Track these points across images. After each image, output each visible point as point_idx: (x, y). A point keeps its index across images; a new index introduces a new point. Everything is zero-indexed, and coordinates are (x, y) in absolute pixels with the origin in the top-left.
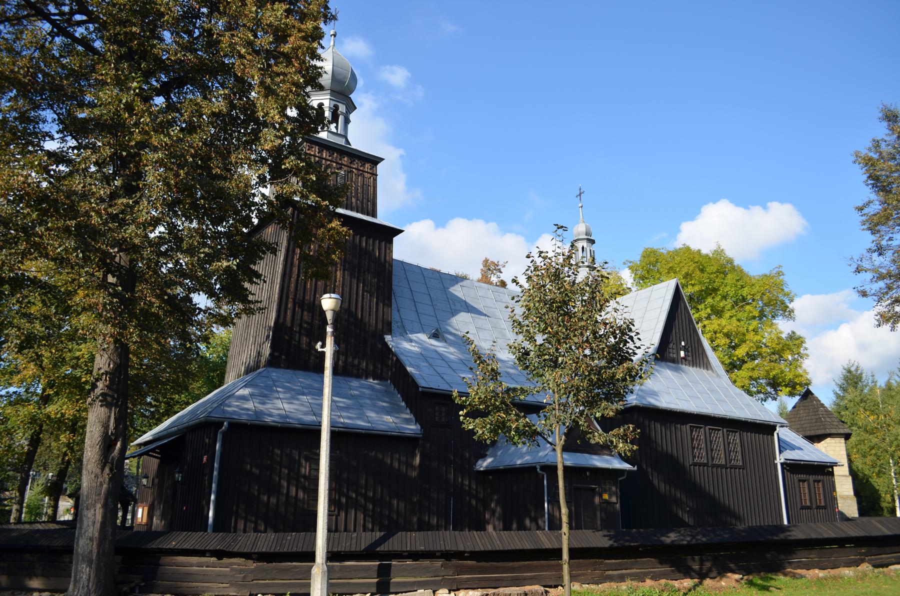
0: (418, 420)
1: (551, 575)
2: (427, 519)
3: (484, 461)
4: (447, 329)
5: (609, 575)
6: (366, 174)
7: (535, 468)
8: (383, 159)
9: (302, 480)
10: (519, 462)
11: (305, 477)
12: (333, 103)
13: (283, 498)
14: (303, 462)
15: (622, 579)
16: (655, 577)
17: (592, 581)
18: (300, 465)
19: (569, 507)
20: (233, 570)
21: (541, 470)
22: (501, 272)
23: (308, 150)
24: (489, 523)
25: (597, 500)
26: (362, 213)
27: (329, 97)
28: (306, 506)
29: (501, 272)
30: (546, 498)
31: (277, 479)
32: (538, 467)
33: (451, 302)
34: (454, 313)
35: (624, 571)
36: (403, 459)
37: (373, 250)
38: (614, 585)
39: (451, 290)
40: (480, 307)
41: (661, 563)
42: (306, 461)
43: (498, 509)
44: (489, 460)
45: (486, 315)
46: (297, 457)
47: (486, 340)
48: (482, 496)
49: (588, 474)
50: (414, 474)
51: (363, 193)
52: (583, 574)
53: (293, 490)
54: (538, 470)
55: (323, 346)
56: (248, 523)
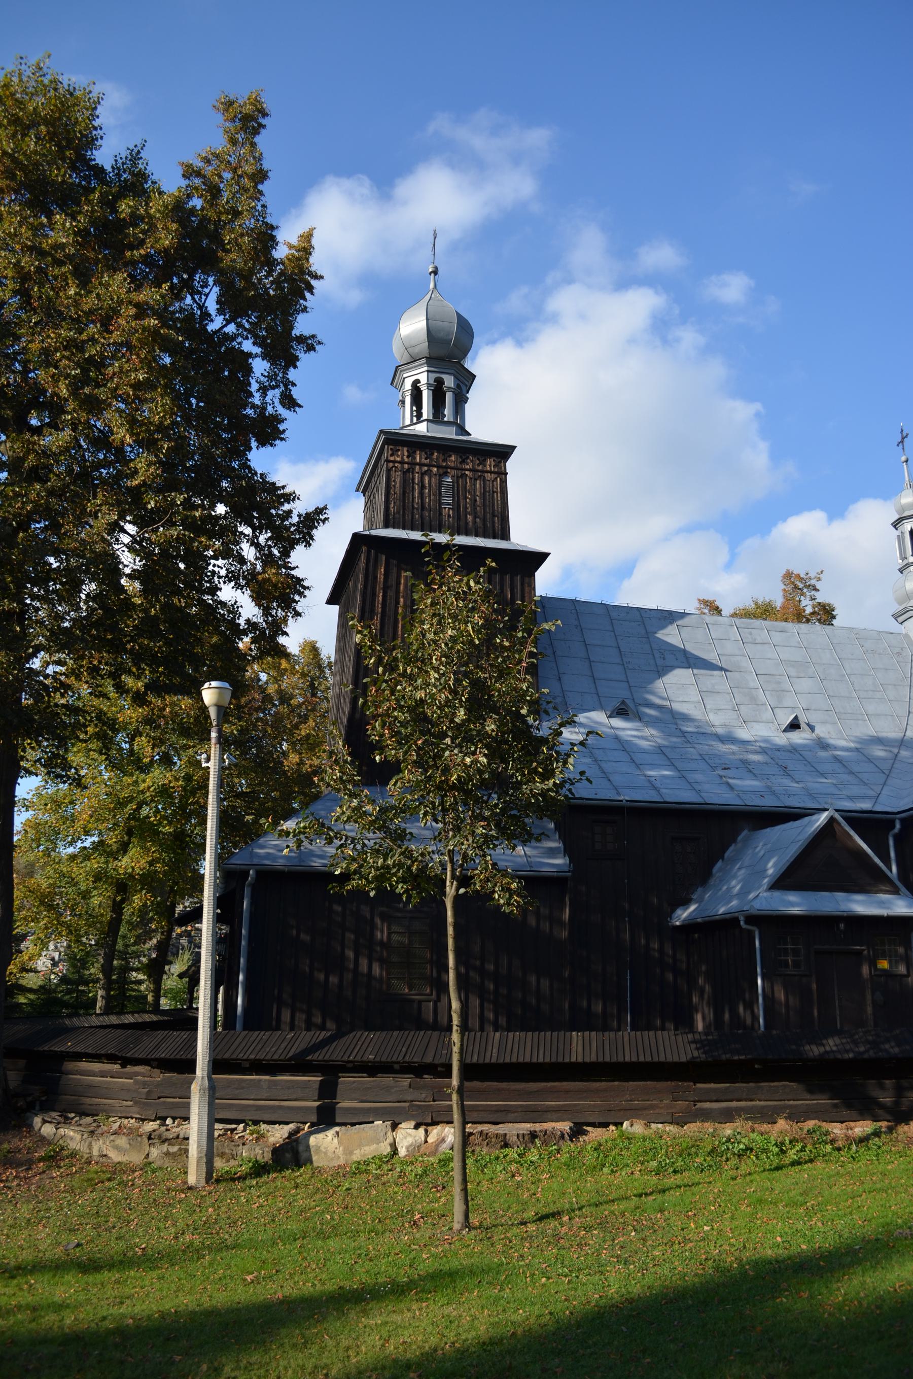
0: (568, 850)
1: (594, 1106)
2: (585, 1004)
3: (687, 909)
4: (646, 700)
5: (701, 1109)
6: (488, 476)
7: (736, 920)
8: (514, 447)
9: (378, 949)
10: (721, 911)
11: (382, 943)
13: (349, 976)
14: (378, 921)
15: (727, 1116)
16: (796, 1116)
17: (669, 1118)
18: (373, 926)
19: (460, 999)
20: (136, 1082)
21: (746, 922)
22: (817, 590)
23: (392, 455)
24: (697, 1011)
25: (865, 970)
26: (485, 536)
27: (426, 368)
28: (384, 987)
29: (817, 590)
30: (759, 970)
31: (339, 949)
32: (742, 919)
33: (657, 655)
34: (662, 671)
35: (734, 1104)
36: (544, 911)
37: (502, 590)
38: (709, 1127)
39: (660, 635)
40: (712, 657)
41: (811, 1092)
42: (383, 920)
43: (708, 988)
44: (692, 908)
45: (721, 669)
46: (368, 916)
47: (717, 710)
48: (684, 966)
49: (842, 926)
50: (564, 934)
51: (484, 505)
52: (652, 1107)
53: (364, 963)
54: (742, 923)
55: (208, 760)
56: (298, 1015)
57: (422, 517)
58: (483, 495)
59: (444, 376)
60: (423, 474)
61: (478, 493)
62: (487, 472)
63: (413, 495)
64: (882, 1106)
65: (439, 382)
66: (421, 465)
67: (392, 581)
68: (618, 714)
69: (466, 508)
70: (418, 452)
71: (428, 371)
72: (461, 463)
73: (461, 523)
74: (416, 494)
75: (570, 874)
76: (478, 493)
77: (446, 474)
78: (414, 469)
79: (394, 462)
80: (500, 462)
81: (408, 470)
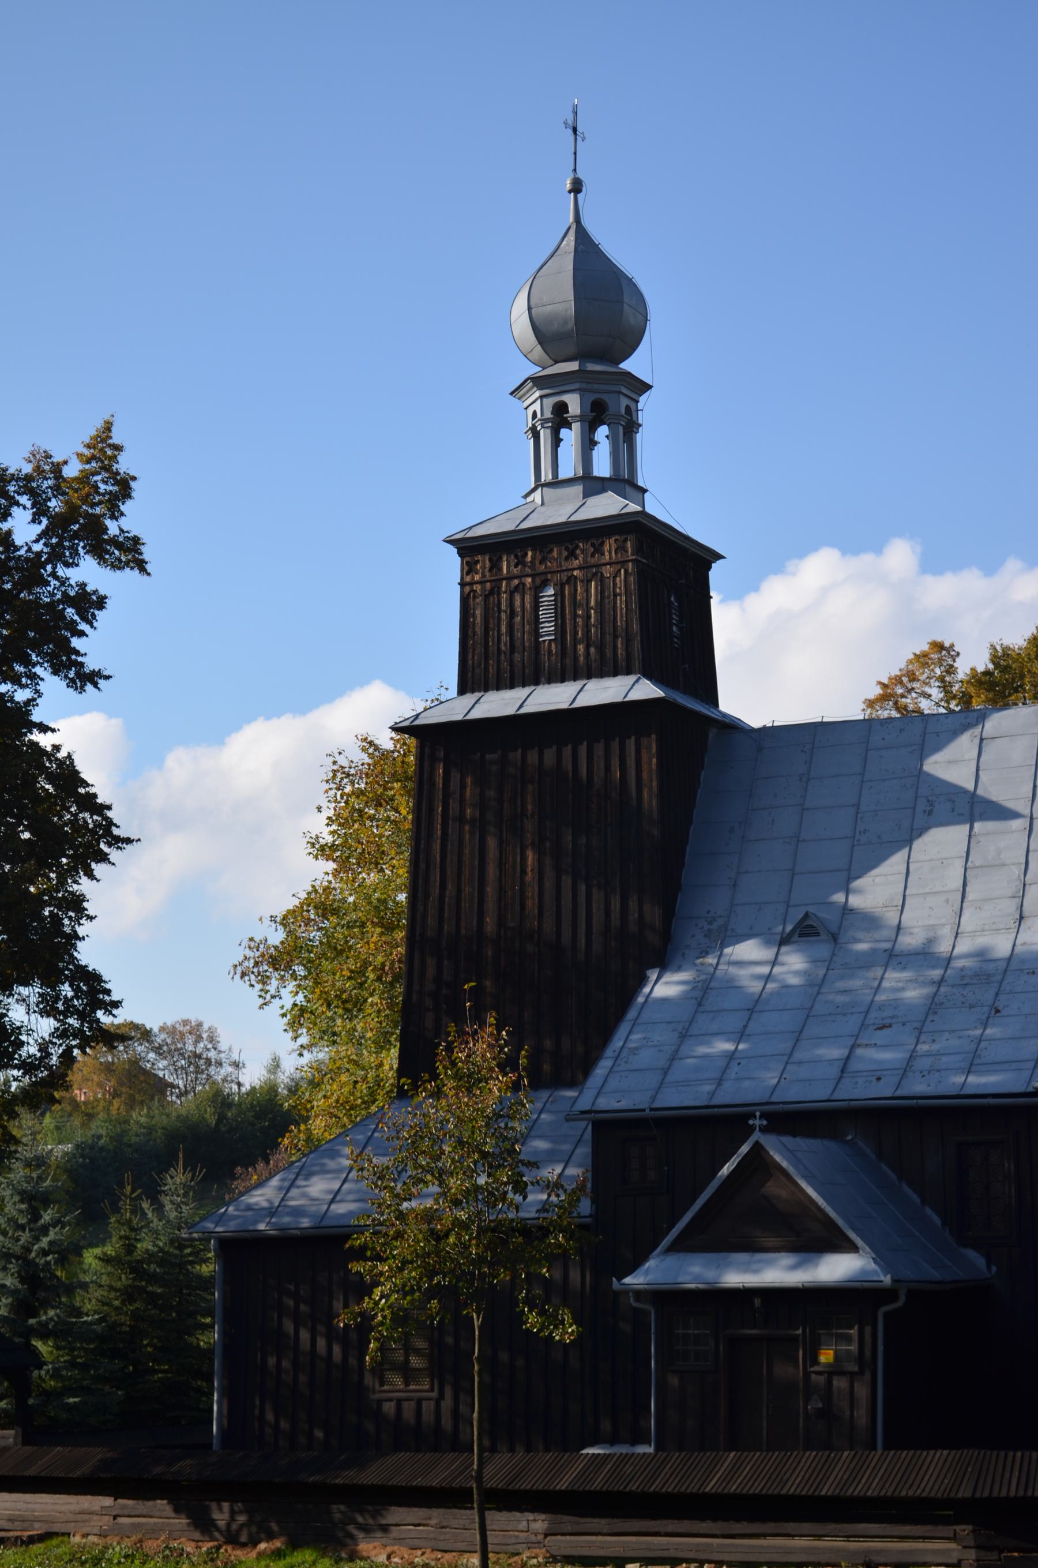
12: (550, 402)
21: (637, 1299)
49: (757, 1302)
51: (601, 621)
57: (511, 663)
58: (600, 604)
59: (567, 398)
61: (593, 603)
62: (605, 564)
63: (499, 631)
64: (218, 1530)
65: (561, 409)
66: (509, 579)
68: (800, 935)
69: (576, 633)
70: (505, 558)
71: (541, 397)
72: (567, 559)
73: (568, 661)
74: (504, 629)
75: (589, 1220)
76: (593, 603)
77: (545, 584)
78: (500, 588)
79: (471, 584)
80: (625, 541)
81: (492, 592)
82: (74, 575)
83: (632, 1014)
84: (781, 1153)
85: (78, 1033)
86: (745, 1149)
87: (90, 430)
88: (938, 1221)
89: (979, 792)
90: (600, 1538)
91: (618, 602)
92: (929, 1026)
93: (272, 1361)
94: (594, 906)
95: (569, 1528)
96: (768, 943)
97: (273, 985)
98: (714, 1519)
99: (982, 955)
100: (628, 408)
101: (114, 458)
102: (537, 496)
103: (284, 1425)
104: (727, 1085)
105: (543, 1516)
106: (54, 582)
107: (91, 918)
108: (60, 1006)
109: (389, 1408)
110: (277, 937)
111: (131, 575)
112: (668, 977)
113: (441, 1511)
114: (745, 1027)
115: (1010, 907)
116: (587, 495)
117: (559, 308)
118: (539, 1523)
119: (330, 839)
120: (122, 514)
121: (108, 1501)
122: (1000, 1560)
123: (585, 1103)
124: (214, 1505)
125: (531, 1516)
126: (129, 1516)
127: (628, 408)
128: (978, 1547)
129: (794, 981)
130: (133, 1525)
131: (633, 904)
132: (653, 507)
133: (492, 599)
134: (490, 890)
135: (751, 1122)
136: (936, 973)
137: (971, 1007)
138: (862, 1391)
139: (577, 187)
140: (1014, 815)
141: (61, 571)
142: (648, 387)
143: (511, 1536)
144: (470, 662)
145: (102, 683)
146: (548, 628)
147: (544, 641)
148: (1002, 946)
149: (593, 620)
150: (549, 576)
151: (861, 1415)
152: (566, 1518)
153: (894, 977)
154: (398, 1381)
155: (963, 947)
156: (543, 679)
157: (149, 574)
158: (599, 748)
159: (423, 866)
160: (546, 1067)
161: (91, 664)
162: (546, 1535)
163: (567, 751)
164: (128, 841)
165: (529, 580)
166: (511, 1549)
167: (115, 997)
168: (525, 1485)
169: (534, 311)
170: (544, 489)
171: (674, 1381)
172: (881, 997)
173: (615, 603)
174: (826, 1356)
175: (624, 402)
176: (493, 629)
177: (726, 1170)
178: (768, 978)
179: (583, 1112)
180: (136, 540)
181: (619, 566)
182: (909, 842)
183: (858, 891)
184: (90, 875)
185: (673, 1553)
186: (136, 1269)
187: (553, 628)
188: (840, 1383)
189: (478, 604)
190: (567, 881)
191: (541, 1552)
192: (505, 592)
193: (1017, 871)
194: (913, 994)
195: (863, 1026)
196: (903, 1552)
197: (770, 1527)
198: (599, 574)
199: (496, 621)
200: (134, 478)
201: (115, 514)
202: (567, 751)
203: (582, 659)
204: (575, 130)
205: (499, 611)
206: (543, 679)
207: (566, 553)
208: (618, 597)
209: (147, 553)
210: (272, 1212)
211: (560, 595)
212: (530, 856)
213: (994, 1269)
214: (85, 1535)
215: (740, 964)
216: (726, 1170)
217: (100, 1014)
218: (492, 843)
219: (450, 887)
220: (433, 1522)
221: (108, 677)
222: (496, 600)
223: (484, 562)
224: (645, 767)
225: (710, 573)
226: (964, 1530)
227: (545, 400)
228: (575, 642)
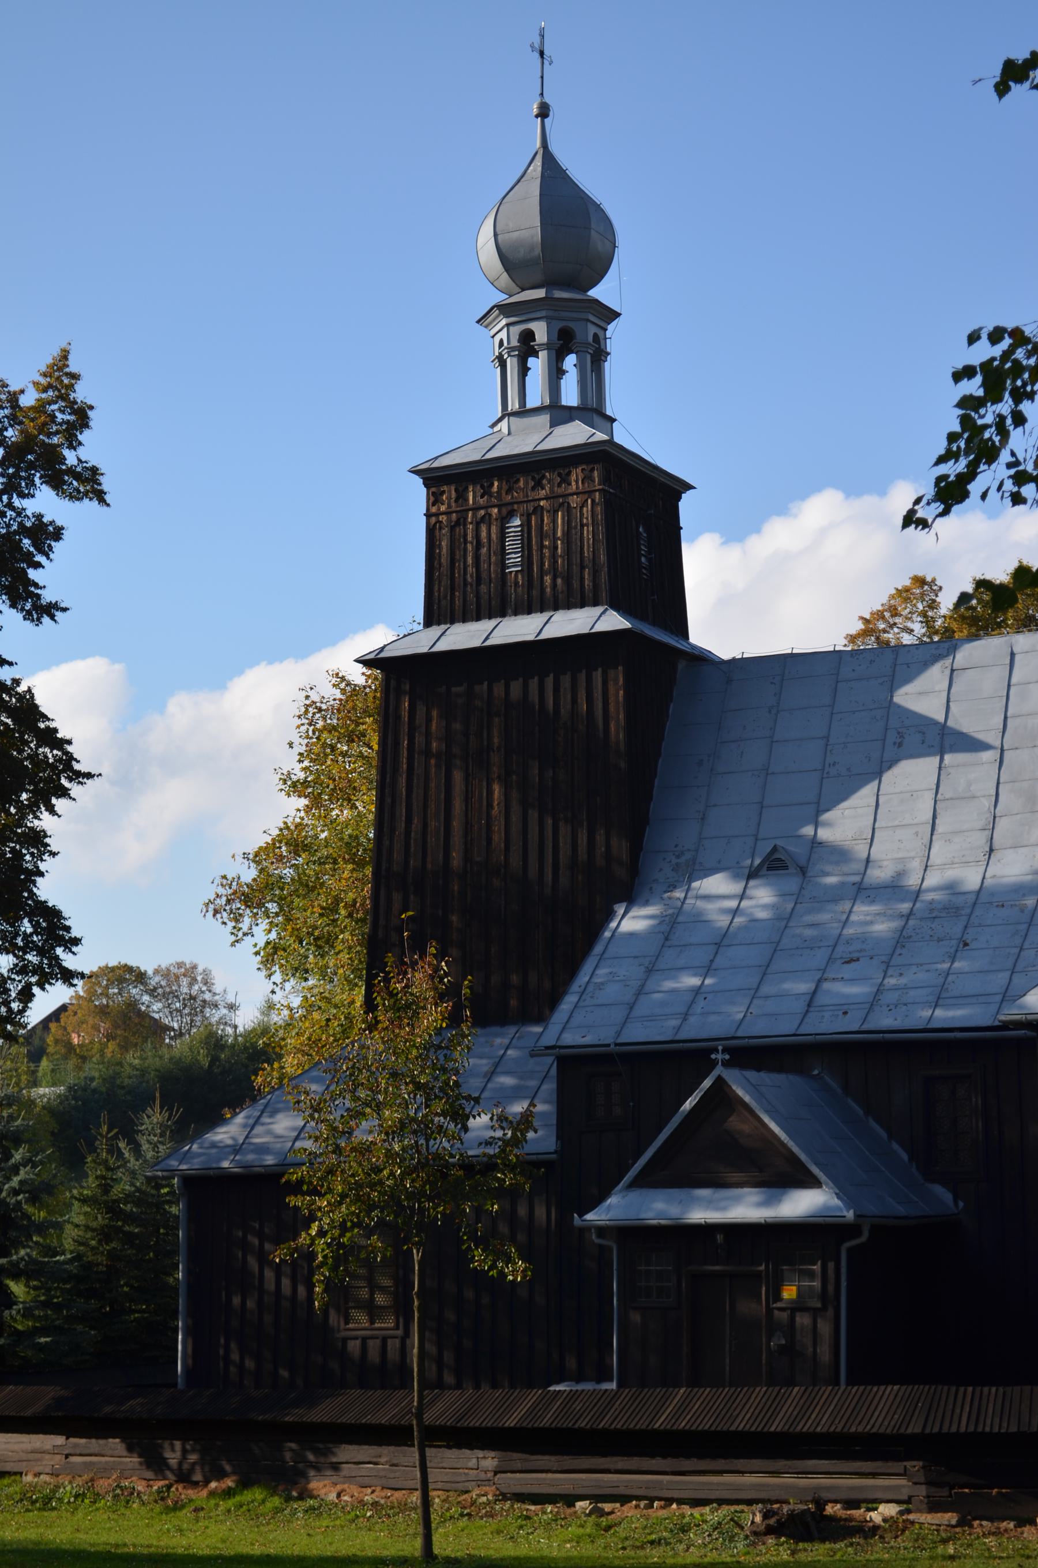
12: (516, 330)
49: (720, 1238)
51: (568, 551)
59: (534, 326)
60: (478, 525)
61: (559, 534)
64: (169, 1468)
65: (527, 337)
66: (475, 509)
67: (420, 719)
68: (769, 869)
69: (542, 564)
70: (471, 489)
71: (508, 325)
72: (533, 489)
74: (470, 560)
76: (559, 534)
77: (511, 514)
78: (466, 519)
79: (437, 515)
80: (592, 470)
81: (458, 523)
82: (31, 506)
83: (598, 949)
84: (744, 1088)
85: (38, 970)
86: (707, 1083)
87: (46, 359)
88: (905, 1157)
89: (950, 723)
90: (550, 1475)
91: (585, 532)
92: (896, 960)
93: (236, 1301)
94: (561, 839)
95: (519, 1466)
96: (736, 877)
97: (246, 923)
98: (664, 1456)
99: (951, 887)
100: (596, 336)
101: (71, 387)
102: (504, 425)
103: (250, 1364)
104: (692, 1019)
105: (493, 1454)
106: (10, 513)
107: (53, 854)
108: (19, 941)
109: (354, 1347)
110: (249, 874)
111: (89, 506)
112: (635, 912)
113: (392, 1448)
114: (712, 961)
115: (980, 839)
116: (554, 424)
117: (525, 234)
118: (489, 1460)
119: (302, 775)
120: (80, 444)
121: (59, 1440)
122: (950, 1496)
123: (549, 1038)
124: (166, 1444)
125: (480, 1454)
126: (81, 1455)
127: (596, 336)
128: (929, 1483)
129: (762, 915)
130: (85, 1463)
131: (600, 838)
132: (621, 438)
133: (458, 530)
134: (457, 824)
135: (713, 1056)
136: (905, 907)
137: (939, 940)
138: (825, 1328)
139: (544, 112)
140: (985, 747)
141: (17, 502)
142: (616, 315)
143: (461, 1474)
144: (436, 594)
145: (59, 615)
146: (514, 559)
147: (511, 572)
148: (971, 879)
149: (559, 551)
150: (516, 507)
151: (825, 1353)
152: (516, 1455)
153: (862, 911)
154: (361, 1318)
155: (933, 880)
156: (510, 611)
157: (108, 505)
158: (566, 681)
159: (389, 800)
160: (513, 1003)
161: (48, 596)
162: (496, 1473)
163: (534, 683)
164: (89, 776)
165: (496, 510)
166: (460, 1487)
167: (74, 933)
168: (475, 1423)
169: (500, 238)
170: (511, 418)
171: (636, 1317)
172: (849, 931)
173: (582, 534)
174: (789, 1293)
175: (592, 330)
176: (459, 561)
177: (688, 1105)
178: (735, 912)
179: (547, 1048)
180: (94, 470)
181: (586, 496)
182: (879, 774)
183: (828, 824)
184: (51, 810)
185: (622, 1491)
186: (112, 1209)
187: (519, 559)
188: (803, 1320)
189: (444, 535)
190: (534, 815)
191: (491, 1490)
192: (471, 523)
193: (987, 803)
194: (882, 928)
195: (830, 960)
196: (852, 1488)
197: (720, 1464)
198: (566, 504)
199: (462, 553)
200: (91, 408)
201: (73, 443)
202: (534, 683)
203: (548, 590)
204: (542, 54)
205: (466, 542)
206: (510, 611)
207: (533, 483)
208: (585, 528)
209: (106, 483)
210: (236, 1149)
211: (526, 525)
212: (497, 790)
213: (961, 1204)
214: (37, 1475)
215: (707, 898)
216: (688, 1105)
217: (59, 951)
218: (458, 776)
219: (416, 821)
220: (383, 1460)
221: (65, 610)
222: (462, 531)
223: (450, 492)
224: (612, 700)
225: (681, 504)
226: (915, 1466)
227: (511, 328)
228: (542, 573)
